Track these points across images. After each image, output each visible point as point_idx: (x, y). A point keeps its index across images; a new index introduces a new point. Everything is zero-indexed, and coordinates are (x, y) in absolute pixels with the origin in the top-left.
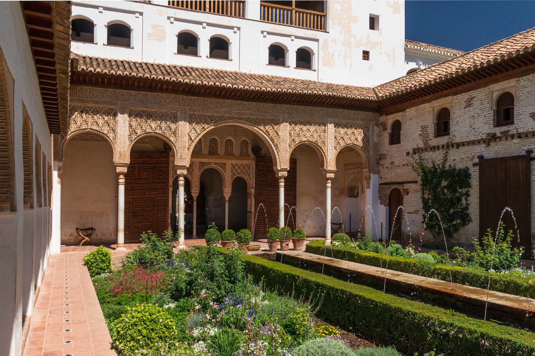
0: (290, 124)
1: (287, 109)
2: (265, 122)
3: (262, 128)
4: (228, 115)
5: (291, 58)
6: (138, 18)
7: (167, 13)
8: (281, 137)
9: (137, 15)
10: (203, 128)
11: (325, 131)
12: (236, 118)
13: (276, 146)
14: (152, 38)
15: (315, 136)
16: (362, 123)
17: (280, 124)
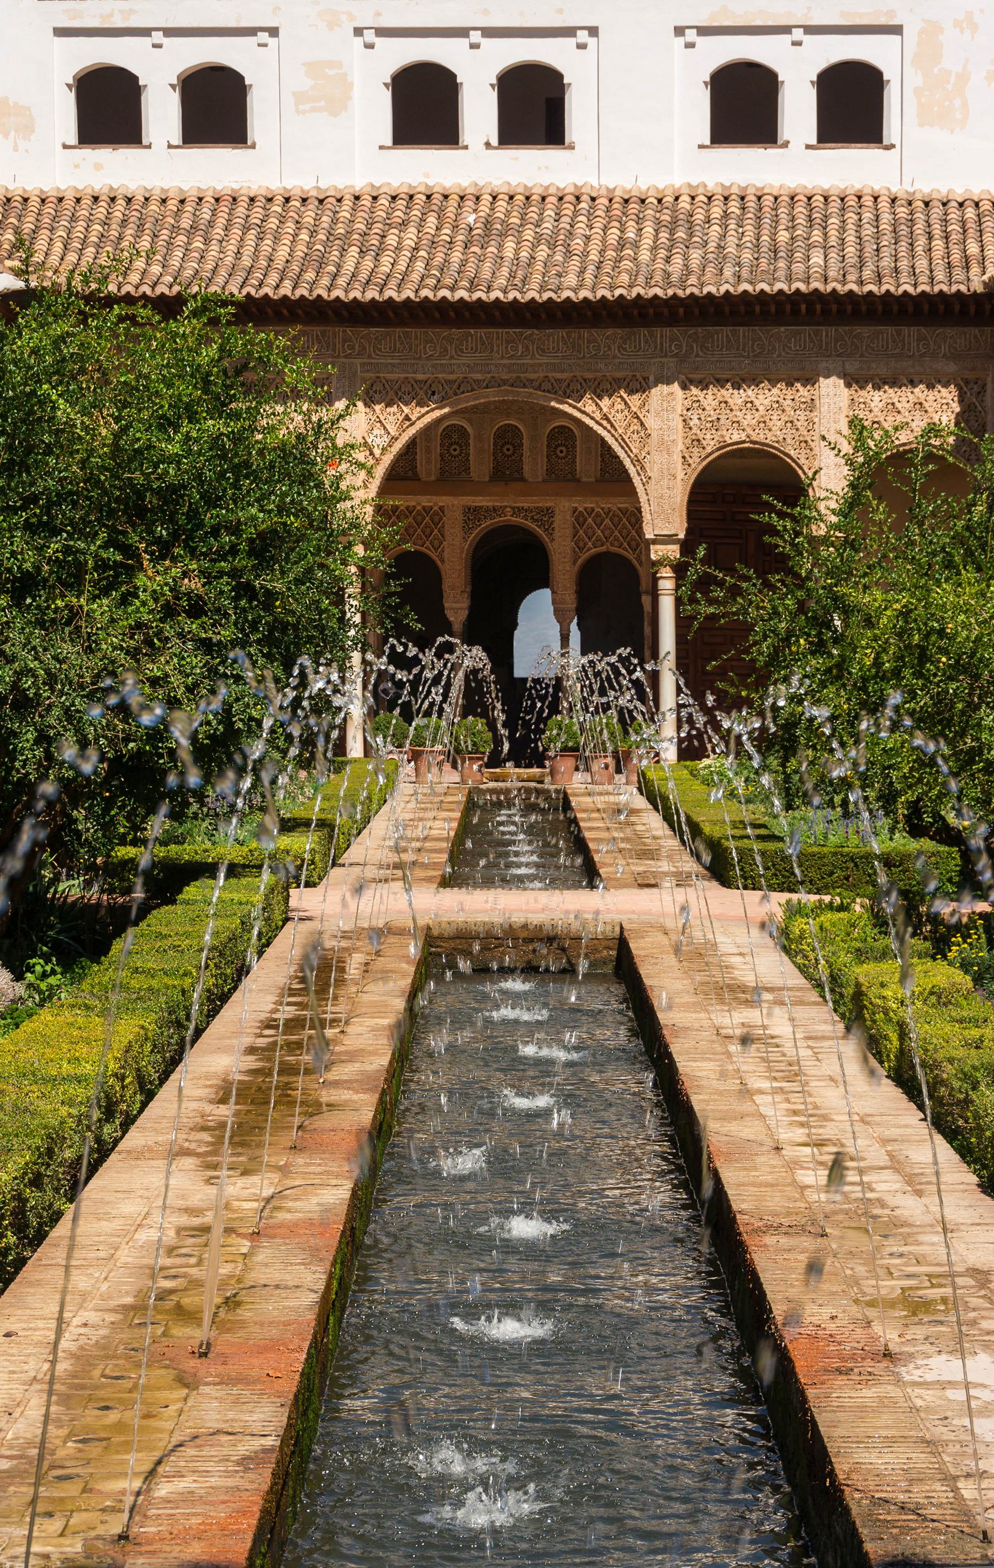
0: (684, 387)
1: (672, 340)
2: (602, 389)
3: (590, 408)
4: (478, 376)
5: (798, 110)
6: (265, 45)
7: (351, 17)
8: (654, 435)
9: (263, 37)
10: (407, 418)
11: (811, 405)
12: (505, 382)
13: (637, 461)
14: (307, 107)
15: (776, 422)
16: (952, 368)
17: (650, 388)
